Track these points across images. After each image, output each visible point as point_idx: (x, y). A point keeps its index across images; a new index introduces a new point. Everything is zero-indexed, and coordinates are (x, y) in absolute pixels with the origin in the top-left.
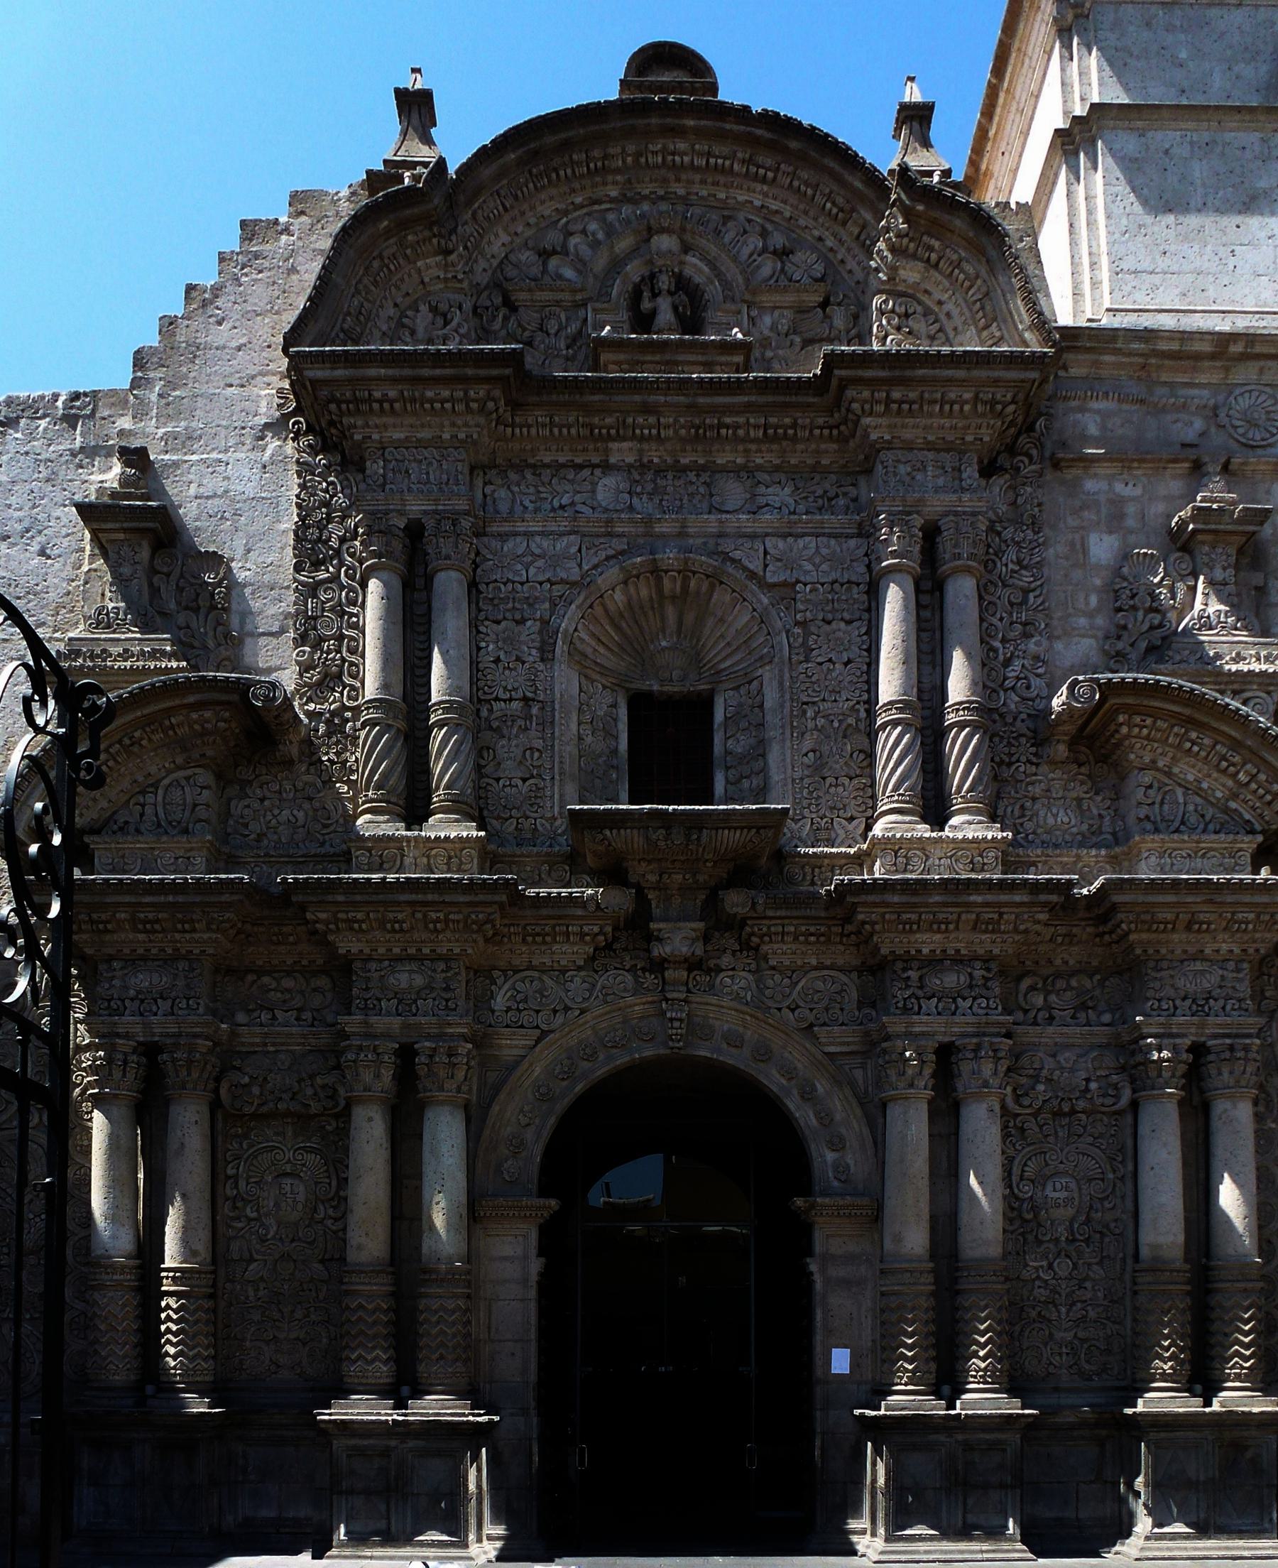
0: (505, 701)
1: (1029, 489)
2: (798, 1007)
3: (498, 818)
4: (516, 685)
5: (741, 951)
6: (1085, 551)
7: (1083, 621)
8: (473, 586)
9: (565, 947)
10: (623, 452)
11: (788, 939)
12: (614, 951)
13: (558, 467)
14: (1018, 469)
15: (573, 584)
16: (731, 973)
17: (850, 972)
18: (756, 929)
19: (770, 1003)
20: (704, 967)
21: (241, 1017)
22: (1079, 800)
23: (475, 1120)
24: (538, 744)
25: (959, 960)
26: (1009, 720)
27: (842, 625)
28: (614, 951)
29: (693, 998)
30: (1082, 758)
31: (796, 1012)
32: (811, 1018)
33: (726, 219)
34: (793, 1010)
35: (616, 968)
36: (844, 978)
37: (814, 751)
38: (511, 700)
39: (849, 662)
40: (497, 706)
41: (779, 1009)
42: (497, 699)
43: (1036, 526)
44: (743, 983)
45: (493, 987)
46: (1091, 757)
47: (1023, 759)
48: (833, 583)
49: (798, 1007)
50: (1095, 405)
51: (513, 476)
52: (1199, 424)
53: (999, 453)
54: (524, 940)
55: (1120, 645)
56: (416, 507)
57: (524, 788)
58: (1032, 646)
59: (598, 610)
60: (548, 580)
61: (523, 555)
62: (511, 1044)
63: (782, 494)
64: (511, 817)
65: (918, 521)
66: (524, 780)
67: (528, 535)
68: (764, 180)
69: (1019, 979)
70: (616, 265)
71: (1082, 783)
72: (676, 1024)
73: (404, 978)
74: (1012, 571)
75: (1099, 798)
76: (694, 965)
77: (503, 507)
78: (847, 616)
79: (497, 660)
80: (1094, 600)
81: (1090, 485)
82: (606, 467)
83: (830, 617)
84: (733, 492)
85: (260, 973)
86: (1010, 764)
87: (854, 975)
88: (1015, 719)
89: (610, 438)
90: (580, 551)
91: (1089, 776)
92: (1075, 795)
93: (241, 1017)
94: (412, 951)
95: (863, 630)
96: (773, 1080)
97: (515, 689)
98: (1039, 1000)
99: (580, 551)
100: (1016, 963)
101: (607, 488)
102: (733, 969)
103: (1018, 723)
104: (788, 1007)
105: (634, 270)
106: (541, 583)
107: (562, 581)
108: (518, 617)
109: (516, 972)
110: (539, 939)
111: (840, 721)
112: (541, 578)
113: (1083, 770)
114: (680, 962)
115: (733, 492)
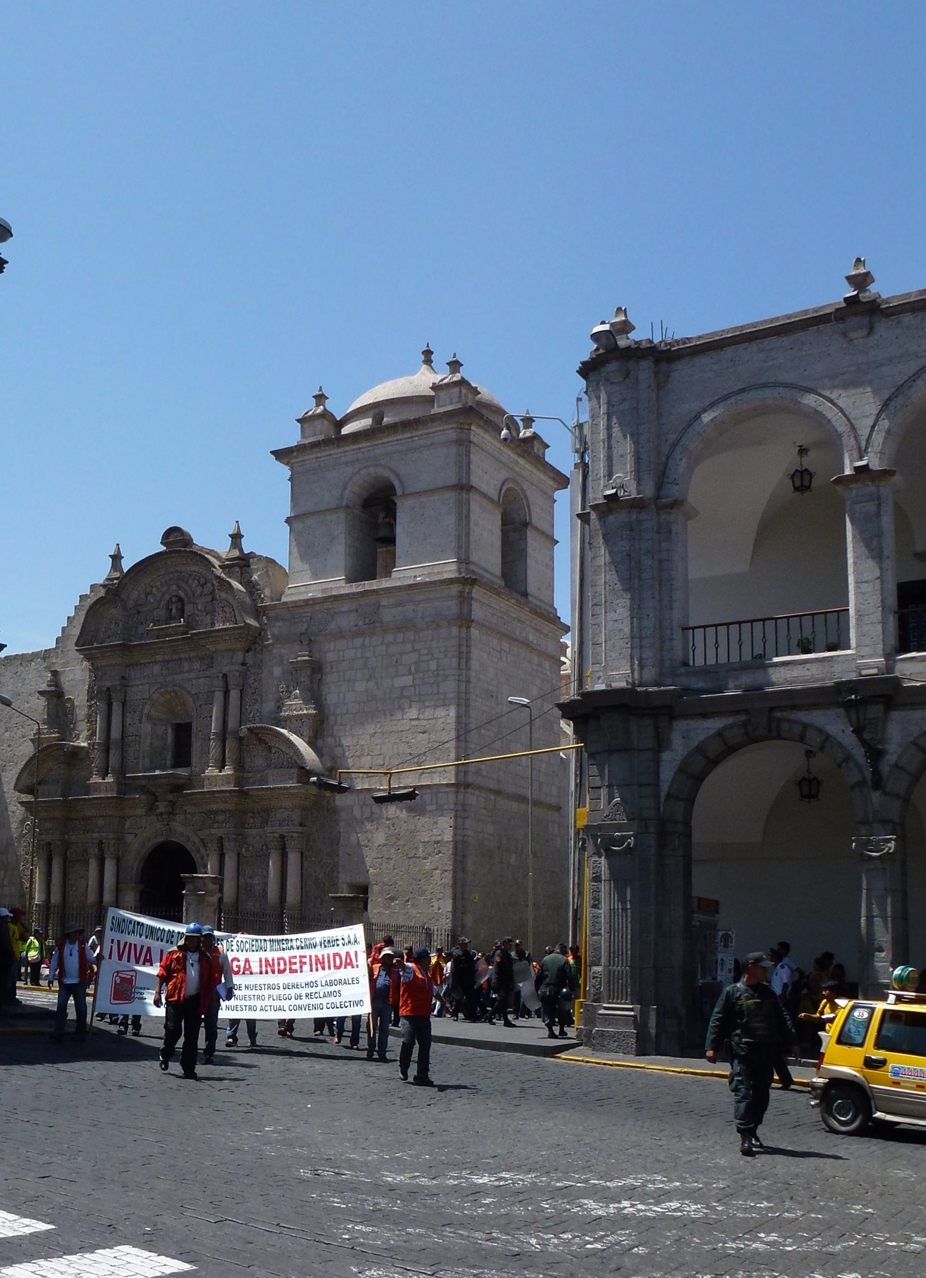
6: (272, 673)
8: (124, 704)
10: (159, 658)
13: (145, 664)
21: (72, 833)
23: (118, 860)
25: (224, 812)
29: (170, 823)
33: (190, 575)
43: (260, 667)
50: (277, 624)
52: (306, 626)
56: (108, 684)
58: (256, 707)
62: (130, 838)
63: (197, 665)
65: (221, 675)
67: (138, 685)
70: (163, 595)
73: (101, 822)
76: (169, 814)
77: (133, 677)
81: (275, 651)
82: (155, 662)
84: (186, 665)
85: (76, 820)
93: (72, 833)
96: (189, 847)
98: (252, 821)
101: (156, 669)
105: (167, 597)
115: (186, 665)
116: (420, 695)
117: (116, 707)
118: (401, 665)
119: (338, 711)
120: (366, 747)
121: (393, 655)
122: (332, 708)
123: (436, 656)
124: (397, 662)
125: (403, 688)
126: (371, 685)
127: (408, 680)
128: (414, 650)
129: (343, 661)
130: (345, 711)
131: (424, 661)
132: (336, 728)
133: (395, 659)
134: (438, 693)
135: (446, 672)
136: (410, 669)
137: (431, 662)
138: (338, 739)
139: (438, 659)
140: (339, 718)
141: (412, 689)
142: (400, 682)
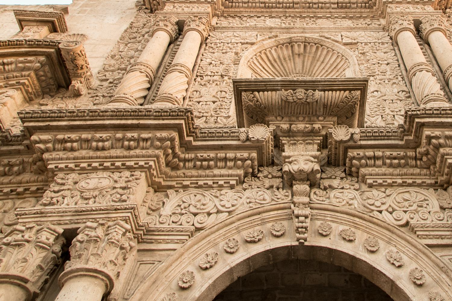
2: (394, 210)
9: (224, 172)
12: (258, 178)
15: (252, 44)
16: (342, 191)
19: (373, 208)
20: (322, 187)
27: (383, 54)
31: (394, 214)
32: (405, 217)
34: (391, 213)
35: (258, 187)
41: (380, 212)
44: (351, 196)
49: (394, 210)
57: (213, 106)
59: (264, 56)
66: (214, 102)
72: (302, 219)
89: (272, 7)
95: (394, 54)
102: (343, 188)
104: (387, 210)
107: (247, 43)
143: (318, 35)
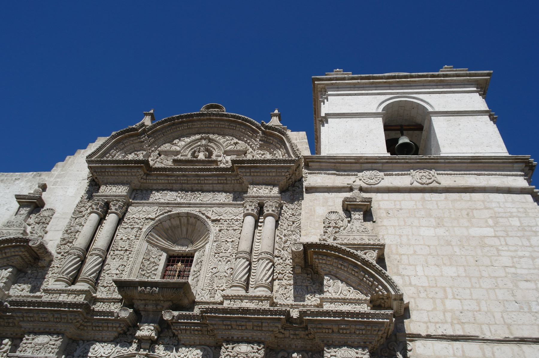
0: (119, 250)
1: (297, 195)
3: (103, 286)
4: (124, 246)
5: (173, 337)
7: (313, 231)
11: (188, 332)
14: (295, 190)
17: (212, 347)
18: (175, 327)
22: (307, 287)
24: (125, 264)
26: (284, 259)
28: (126, 335)
30: (309, 272)
36: (209, 350)
37: (215, 268)
38: (121, 250)
39: (233, 241)
40: (116, 252)
42: (117, 250)
45: (78, 347)
46: (312, 272)
47: (288, 272)
48: (232, 219)
51: (144, 192)
53: (289, 187)
54: (92, 329)
55: (324, 237)
60: (145, 218)
61: (140, 211)
64: (108, 286)
68: (233, 129)
69: (278, 353)
71: (308, 280)
74: (290, 216)
75: (314, 286)
78: (235, 228)
79: (122, 239)
80: (317, 225)
83: (228, 228)
86: (282, 274)
87: (213, 348)
88: (286, 259)
90: (157, 210)
91: (312, 279)
92: (305, 284)
94: (47, 330)
95: (239, 232)
97: (124, 247)
99: (157, 210)
100: (276, 346)
102: (168, 344)
103: (287, 260)
106: (143, 219)
107: (149, 218)
108: (132, 227)
109: (88, 341)
110: (97, 329)
111: (226, 259)
112: (142, 217)
113: (309, 276)
114: (147, 340)
116: (507, 244)
117: (111, 219)
118: (474, 218)
119: (401, 251)
120: (449, 290)
121: (462, 209)
122: (394, 248)
123: (514, 214)
124: (468, 214)
125: (482, 238)
126: (441, 231)
127: (489, 232)
128: (487, 208)
129: (401, 209)
130: (412, 252)
131: (502, 217)
132: (401, 267)
133: (466, 213)
134: (531, 246)
135: (534, 229)
136: (486, 222)
137: (510, 219)
138: (407, 278)
139: (519, 217)
140: (404, 258)
141: (496, 240)
142: (475, 232)
143: (198, 209)
